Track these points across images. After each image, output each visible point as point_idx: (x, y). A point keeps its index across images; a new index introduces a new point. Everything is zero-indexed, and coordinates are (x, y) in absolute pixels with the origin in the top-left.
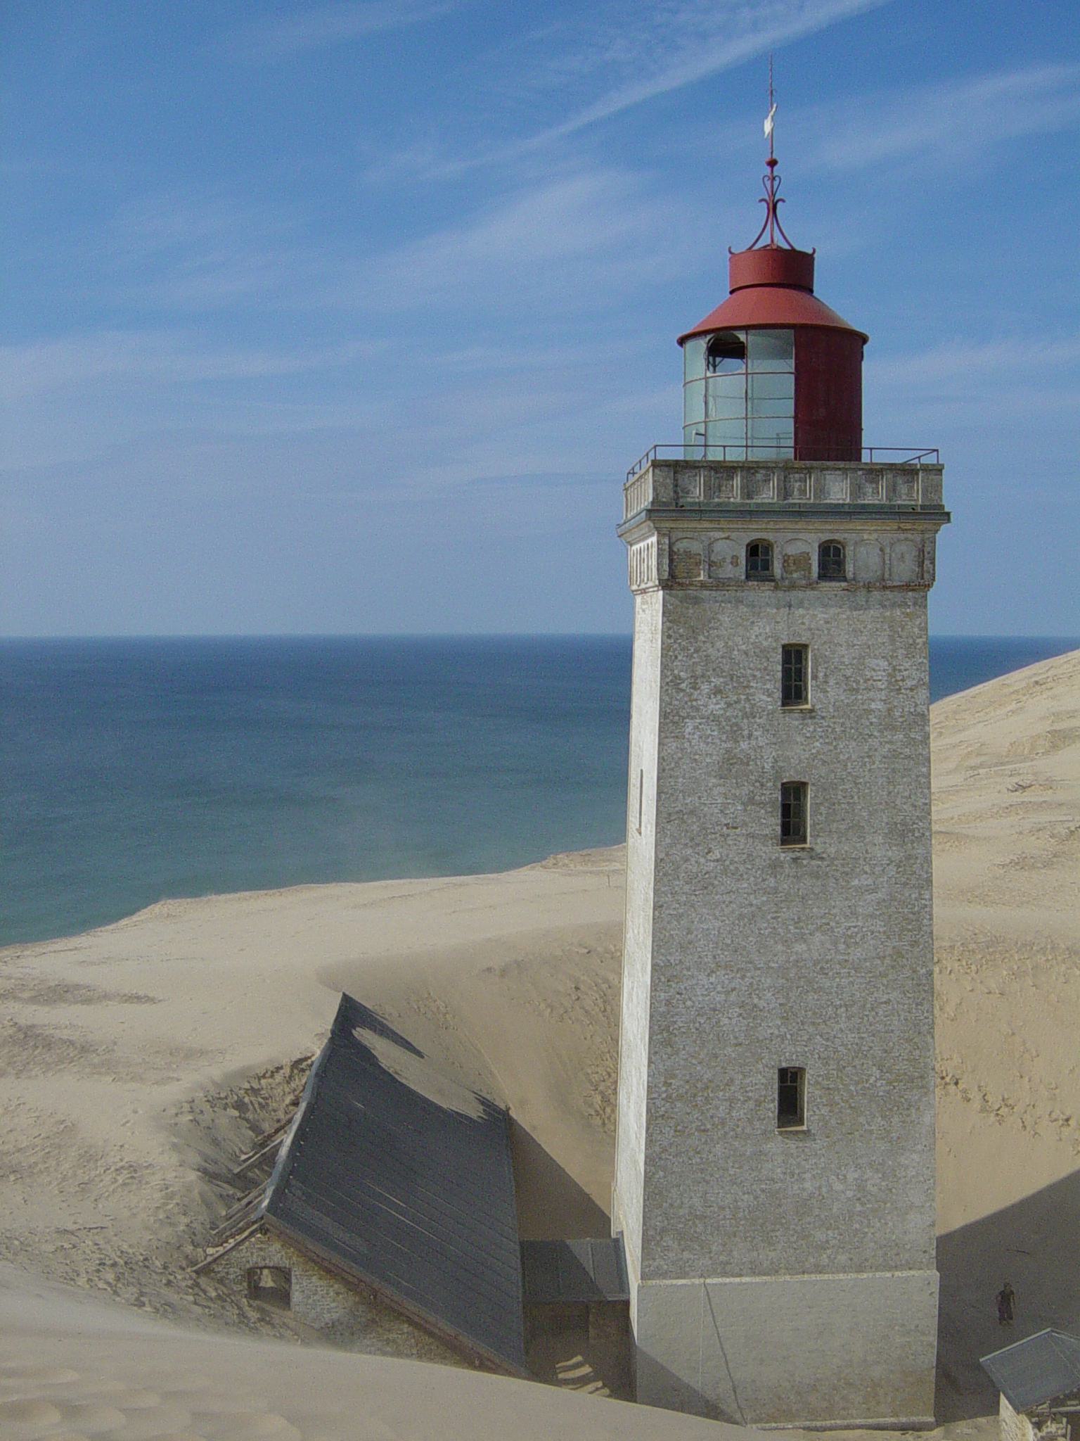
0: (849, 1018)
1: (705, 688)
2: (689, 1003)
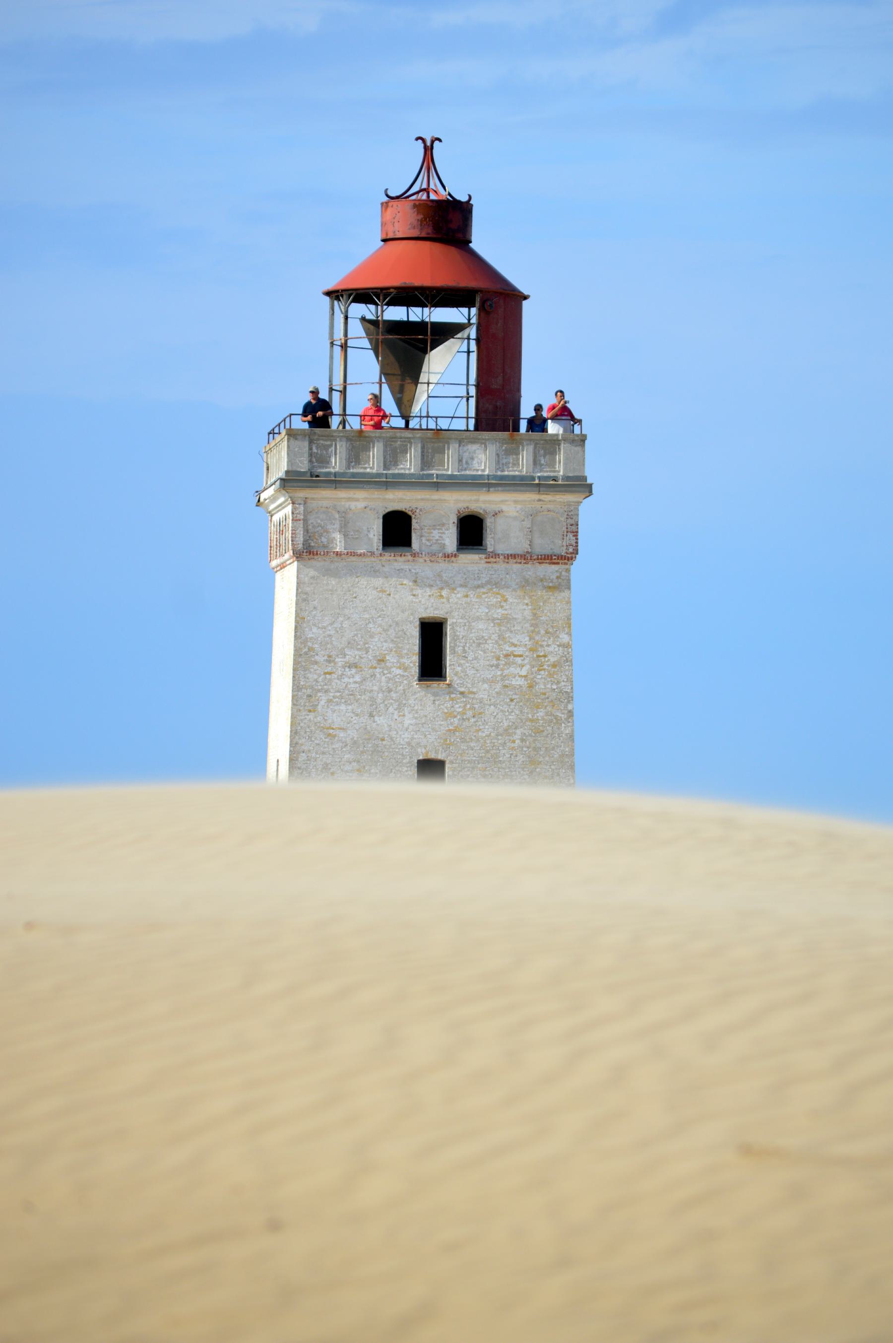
1: (340, 661)
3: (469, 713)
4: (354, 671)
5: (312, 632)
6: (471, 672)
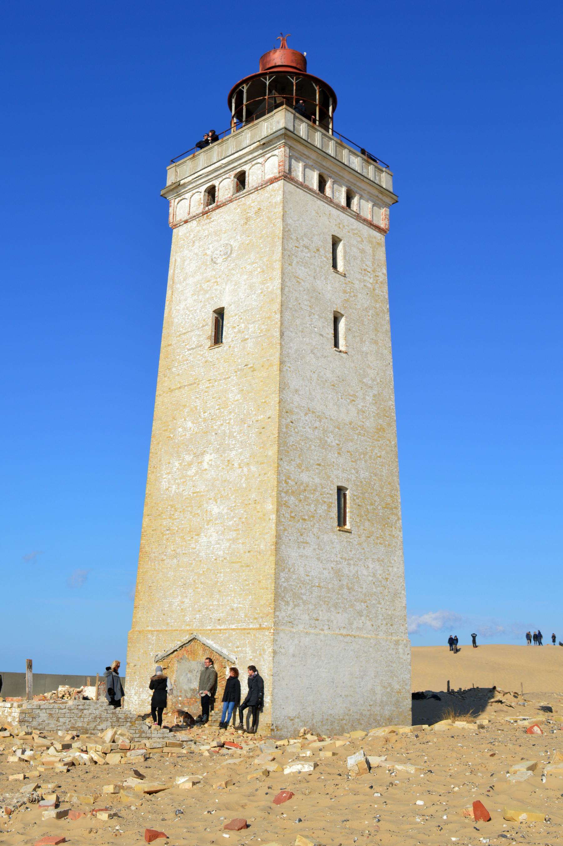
0: (366, 461)
2: (296, 430)
3: (352, 294)
4: (307, 250)
5: (290, 221)
6: (352, 272)
